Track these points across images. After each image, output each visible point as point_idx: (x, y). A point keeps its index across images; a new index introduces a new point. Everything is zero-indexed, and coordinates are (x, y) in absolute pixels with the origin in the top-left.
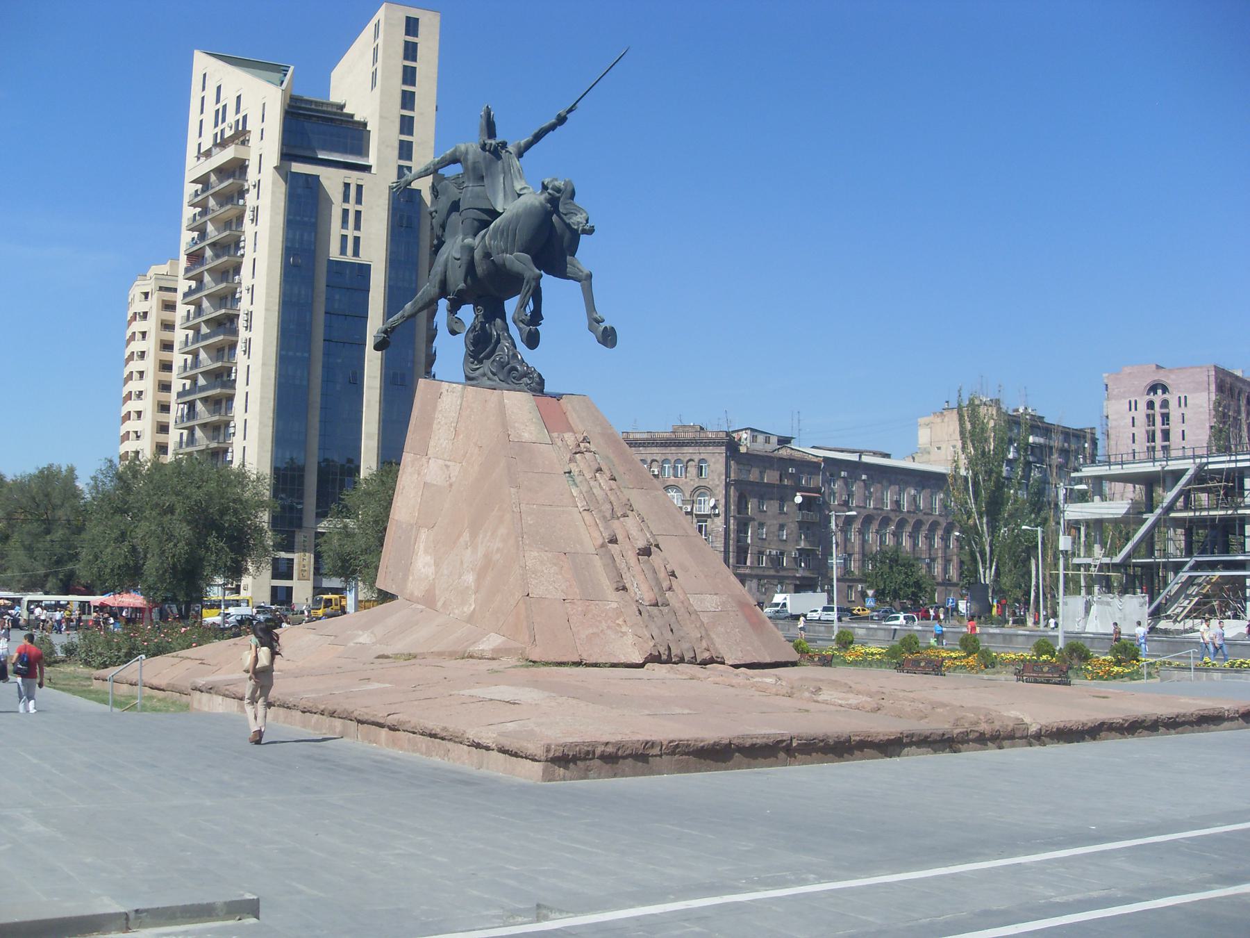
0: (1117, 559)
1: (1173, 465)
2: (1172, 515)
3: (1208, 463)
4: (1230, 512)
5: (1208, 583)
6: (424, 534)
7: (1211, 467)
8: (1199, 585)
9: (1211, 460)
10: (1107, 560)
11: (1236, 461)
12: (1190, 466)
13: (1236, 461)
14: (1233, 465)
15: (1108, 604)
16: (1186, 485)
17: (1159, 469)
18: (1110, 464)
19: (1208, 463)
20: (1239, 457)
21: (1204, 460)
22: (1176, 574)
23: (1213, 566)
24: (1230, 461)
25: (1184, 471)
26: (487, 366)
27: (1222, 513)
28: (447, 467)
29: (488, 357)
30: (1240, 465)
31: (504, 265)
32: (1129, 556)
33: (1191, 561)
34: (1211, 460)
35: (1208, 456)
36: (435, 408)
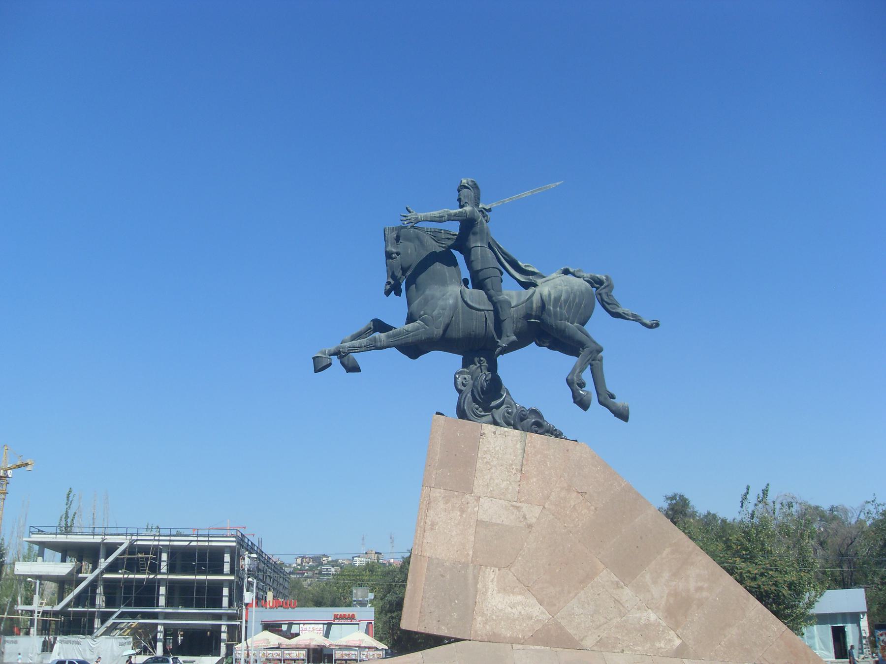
0: (58, 608)
1: (110, 539)
2: (105, 576)
3: (137, 540)
4: (152, 576)
5: (129, 628)
6: (491, 576)
7: (139, 543)
8: (121, 629)
9: (139, 538)
10: (48, 608)
11: (159, 540)
12: (125, 541)
13: (159, 540)
14: (156, 543)
15: (78, 643)
16: (121, 554)
17: (100, 541)
18: (94, 534)
19: (137, 540)
20: (161, 538)
21: (134, 538)
22: (103, 623)
23: (133, 616)
24: (155, 540)
25: (121, 544)
26: (498, 414)
27: (121, 576)
28: (518, 508)
29: (498, 407)
30: (161, 543)
31: (564, 331)
32: (68, 605)
33: (118, 611)
34: (139, 538)
35: (137, 535)
36: (476, 447)
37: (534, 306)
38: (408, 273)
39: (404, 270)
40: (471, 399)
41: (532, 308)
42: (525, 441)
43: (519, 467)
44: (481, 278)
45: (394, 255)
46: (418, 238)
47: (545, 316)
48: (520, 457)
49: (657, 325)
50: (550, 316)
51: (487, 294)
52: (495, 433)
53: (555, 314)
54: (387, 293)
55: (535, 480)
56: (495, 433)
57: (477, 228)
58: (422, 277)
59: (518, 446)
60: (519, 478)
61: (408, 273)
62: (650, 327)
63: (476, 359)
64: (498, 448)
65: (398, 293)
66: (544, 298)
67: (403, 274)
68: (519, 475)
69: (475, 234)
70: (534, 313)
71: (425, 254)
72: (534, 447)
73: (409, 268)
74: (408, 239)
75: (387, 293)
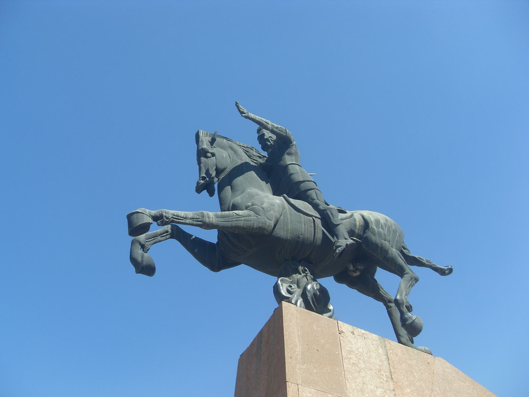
37: (358, 224)
38: (222, 176)
39: (219, 171)
40: (303, 304)
41: (355, 225)
42: (385, 347)
43: (388, 374)
44: (303, 189)
45: (209, 155)
46: (232, 148)
47: (369, 234)
48: (386, 363)
49: (451, 270)
50: (374, 235)
51: (310, 203)
52: (353, 333)
53: (380, 234)
54: (199, 189)
55: (408, 390)
56: (353, 333)
57: (293, 150)
58: (239, 180)
59: (380, 351)
60: (392, 387)
61: (222, 176)
62: (442, 272)
63: (301, 268)
64: (361, 350)
65: (211, 194)
67: (217, 175)
68: (391, 382)
69: (290, 154)
70: (357, 231)
71: (240, 162)
72: (397, 355)
73: (223, 170)
74: (223, 147)
75: (199, 189)
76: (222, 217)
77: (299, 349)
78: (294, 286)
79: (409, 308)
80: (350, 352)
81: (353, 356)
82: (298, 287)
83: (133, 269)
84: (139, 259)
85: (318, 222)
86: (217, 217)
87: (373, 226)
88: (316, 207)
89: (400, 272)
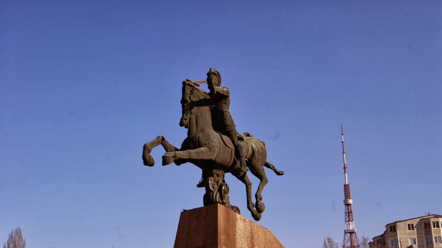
36: (234, 225)
49: (282, 174)
52: (241, 219)
56: (241, 219)
62: (278, 174)
66: (254, 149)
69: (225, 104)
76: (197, 153)
77: (222, 228)
78: (216, 185)
79: (261, 199)
80: (239, 229)
81: (239, 231)
82: (218, 185)
83: (142, 161)
84: (148, 159)
85: (234, 152)
86: (195, 153)
87: (256, 154)
88: (233, 142)
89: (260, 176)
